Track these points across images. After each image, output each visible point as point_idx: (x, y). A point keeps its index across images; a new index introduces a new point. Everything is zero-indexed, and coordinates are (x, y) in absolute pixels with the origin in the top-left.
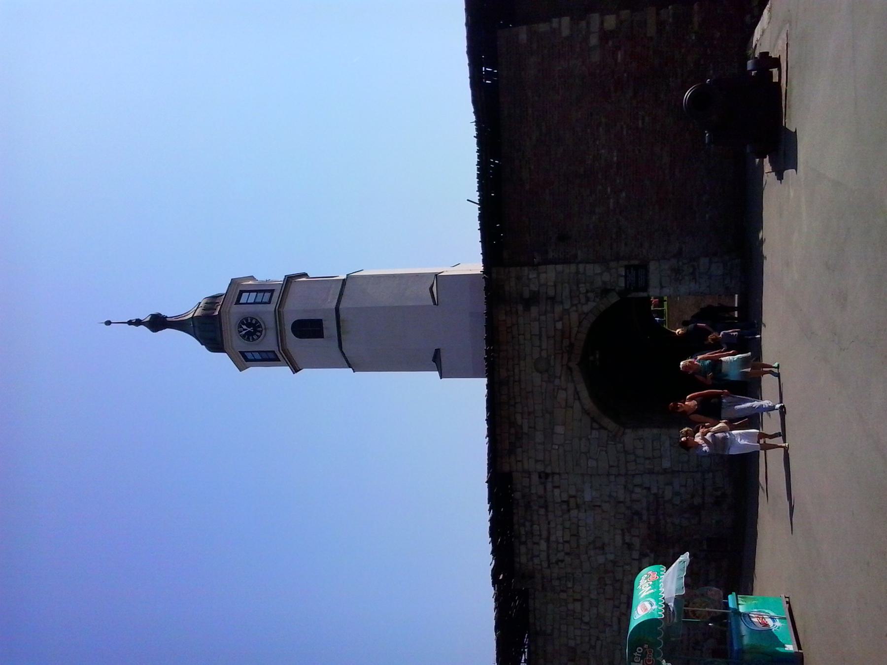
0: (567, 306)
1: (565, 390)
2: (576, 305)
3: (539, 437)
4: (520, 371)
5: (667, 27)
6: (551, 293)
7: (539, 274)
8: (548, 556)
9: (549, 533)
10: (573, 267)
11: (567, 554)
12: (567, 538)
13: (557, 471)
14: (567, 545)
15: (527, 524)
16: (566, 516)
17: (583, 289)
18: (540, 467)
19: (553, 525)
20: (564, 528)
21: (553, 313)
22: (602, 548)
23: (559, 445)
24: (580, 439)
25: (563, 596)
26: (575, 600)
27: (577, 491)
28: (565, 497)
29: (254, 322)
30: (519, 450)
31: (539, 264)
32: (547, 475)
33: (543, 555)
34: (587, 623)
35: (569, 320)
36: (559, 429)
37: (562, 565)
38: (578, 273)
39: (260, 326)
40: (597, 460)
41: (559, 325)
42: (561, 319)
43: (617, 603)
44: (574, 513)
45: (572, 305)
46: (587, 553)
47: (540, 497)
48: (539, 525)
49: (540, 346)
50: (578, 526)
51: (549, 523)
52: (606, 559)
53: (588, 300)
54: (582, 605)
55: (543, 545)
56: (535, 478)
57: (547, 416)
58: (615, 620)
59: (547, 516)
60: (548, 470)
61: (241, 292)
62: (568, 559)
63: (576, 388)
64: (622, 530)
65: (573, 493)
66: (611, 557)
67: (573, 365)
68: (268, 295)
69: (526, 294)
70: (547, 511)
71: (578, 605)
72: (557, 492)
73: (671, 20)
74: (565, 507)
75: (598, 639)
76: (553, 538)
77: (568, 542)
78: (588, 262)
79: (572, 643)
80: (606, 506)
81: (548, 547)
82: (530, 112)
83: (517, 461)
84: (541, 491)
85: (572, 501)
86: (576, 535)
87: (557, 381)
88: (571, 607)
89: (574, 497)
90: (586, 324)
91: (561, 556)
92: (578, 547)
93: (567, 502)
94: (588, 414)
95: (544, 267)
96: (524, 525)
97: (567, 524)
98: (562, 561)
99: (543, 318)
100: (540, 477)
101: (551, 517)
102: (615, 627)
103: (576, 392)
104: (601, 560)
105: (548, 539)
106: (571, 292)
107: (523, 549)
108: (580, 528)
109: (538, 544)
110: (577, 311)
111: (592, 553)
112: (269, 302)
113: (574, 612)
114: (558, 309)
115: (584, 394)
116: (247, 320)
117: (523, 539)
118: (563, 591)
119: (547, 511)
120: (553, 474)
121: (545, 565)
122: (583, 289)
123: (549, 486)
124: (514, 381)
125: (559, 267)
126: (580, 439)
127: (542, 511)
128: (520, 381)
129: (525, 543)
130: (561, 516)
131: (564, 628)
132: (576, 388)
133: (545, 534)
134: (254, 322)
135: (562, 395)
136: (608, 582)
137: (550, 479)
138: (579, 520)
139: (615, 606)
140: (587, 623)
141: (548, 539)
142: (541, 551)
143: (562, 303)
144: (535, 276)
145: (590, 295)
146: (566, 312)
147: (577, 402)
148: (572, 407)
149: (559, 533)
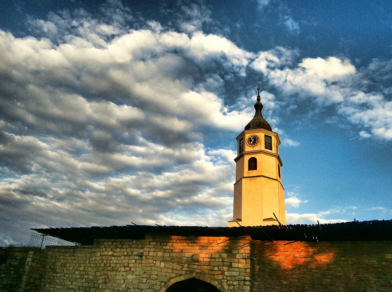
0: (226, 273)
1: (182, 270)
2: (227, 279)
3: (160, 254)
6: (234, 265)
7: (245, 259)
8: (105, 255)
9: (117, 256)
10: (248, 278)
11: (105, 265)
12: (112, 265)
13: (143, 262)
14: (109, 264)
15: (121, 246)
16: (122, 265)
17: (235, 283)
18: (145, 254)
19: (119, 258)
20: (116, 264)
21: (224, 266)
22: (106, 283)
23: (155, 264)
24: (157, 275)
25: (87, 262)
26: (85, 267)
27: (133, 272)
28: (131, 265)
29: (256, 142)
30: (154, 243)
31: (252, 260)
32: (141, 256)
33: (106, 253)
34: (74, 273)
35: (218, 274)
36: (163, 265)
37: (100, 262)
38: (245, 281)
39: (254, 144)
40: (146, 283)
41: (216, 268)
42: (219, 270)
43: (80, 288)
44: (123, 269)
45: (227, 276)
46: (104, 274)
47: (132, 252)
48: (120, 252)
49: (206, 258)
50: (116, 271)
51: (120, 257)
52: (100, 284)
53: (229, 285)
54: (82, 271)
55: (111, 253)
56: (141, 251)
57: (169, 259)
58: (74, 287)
60: (144, 257)
61: (271, 137)
62: (102, 265)
63: (181, 275)
65: (133, 269)
66: (101, 286)
67: (194, 275)
69: (234, 252)
70: (126, 256)
71: (82, 269)
72: (134, 261)
74: (126, 265)
75: (67, 278)
76: (113, 258)
77: (110, 266)
78: (251, 287)
79: (68, 265)
80: (124, 286)
81: (109, 255)
82: (343, 259)
83: (149, 242)
84: (135, 253)
85: (128, 269)
86: (113, 270)
87: (186, 265)
88: (82, 265)
89: (130, 270)
91: (105, 262)
92: (108, 270)
93: (128, 266)
94: (168, 281)
95: (249, 262)
96: (120, 245)
97: (118, 266)
98: (102, 262)
99: (221, 260)
100: (142, 253)
101: (123, 257)
102: (71, 287)
103: (180, 275)
104: (100, 281)
105: (112, 255)
106: (235, 276)
107: (110, 243)
108: (115, 272)
109: (111, 250)
110: (223, 279)
111: (103, 277)
113: (80, 267)
114: (225, 268)
115: (178, 279)
116: (257, 139)
117: (115, 244)
118: (89, 261)
119: (126, 256)
120: (142, 260)
121: (102, 254)
122: (235, 283)
123: (137, 258)
124: (188, 243)
125: (248, 271)
126: (157, 275)
127: (126, 253)
129: (113, 244)
130: (122, 263)
131: (74, 262)
133: (115, 254)
135: (179, 267)
136: (90, 284)
137: (140, 258)
138: (119, 271)
139: (79, 287)
140: (74, 273)
141: (112, 255)
142: (108, 252)
143: (228, 271)
144: (244, 257)
145: (232, 287)
146: (223, 273)
147: (174, 275)
148: (173, 273)
149: (115, 261)
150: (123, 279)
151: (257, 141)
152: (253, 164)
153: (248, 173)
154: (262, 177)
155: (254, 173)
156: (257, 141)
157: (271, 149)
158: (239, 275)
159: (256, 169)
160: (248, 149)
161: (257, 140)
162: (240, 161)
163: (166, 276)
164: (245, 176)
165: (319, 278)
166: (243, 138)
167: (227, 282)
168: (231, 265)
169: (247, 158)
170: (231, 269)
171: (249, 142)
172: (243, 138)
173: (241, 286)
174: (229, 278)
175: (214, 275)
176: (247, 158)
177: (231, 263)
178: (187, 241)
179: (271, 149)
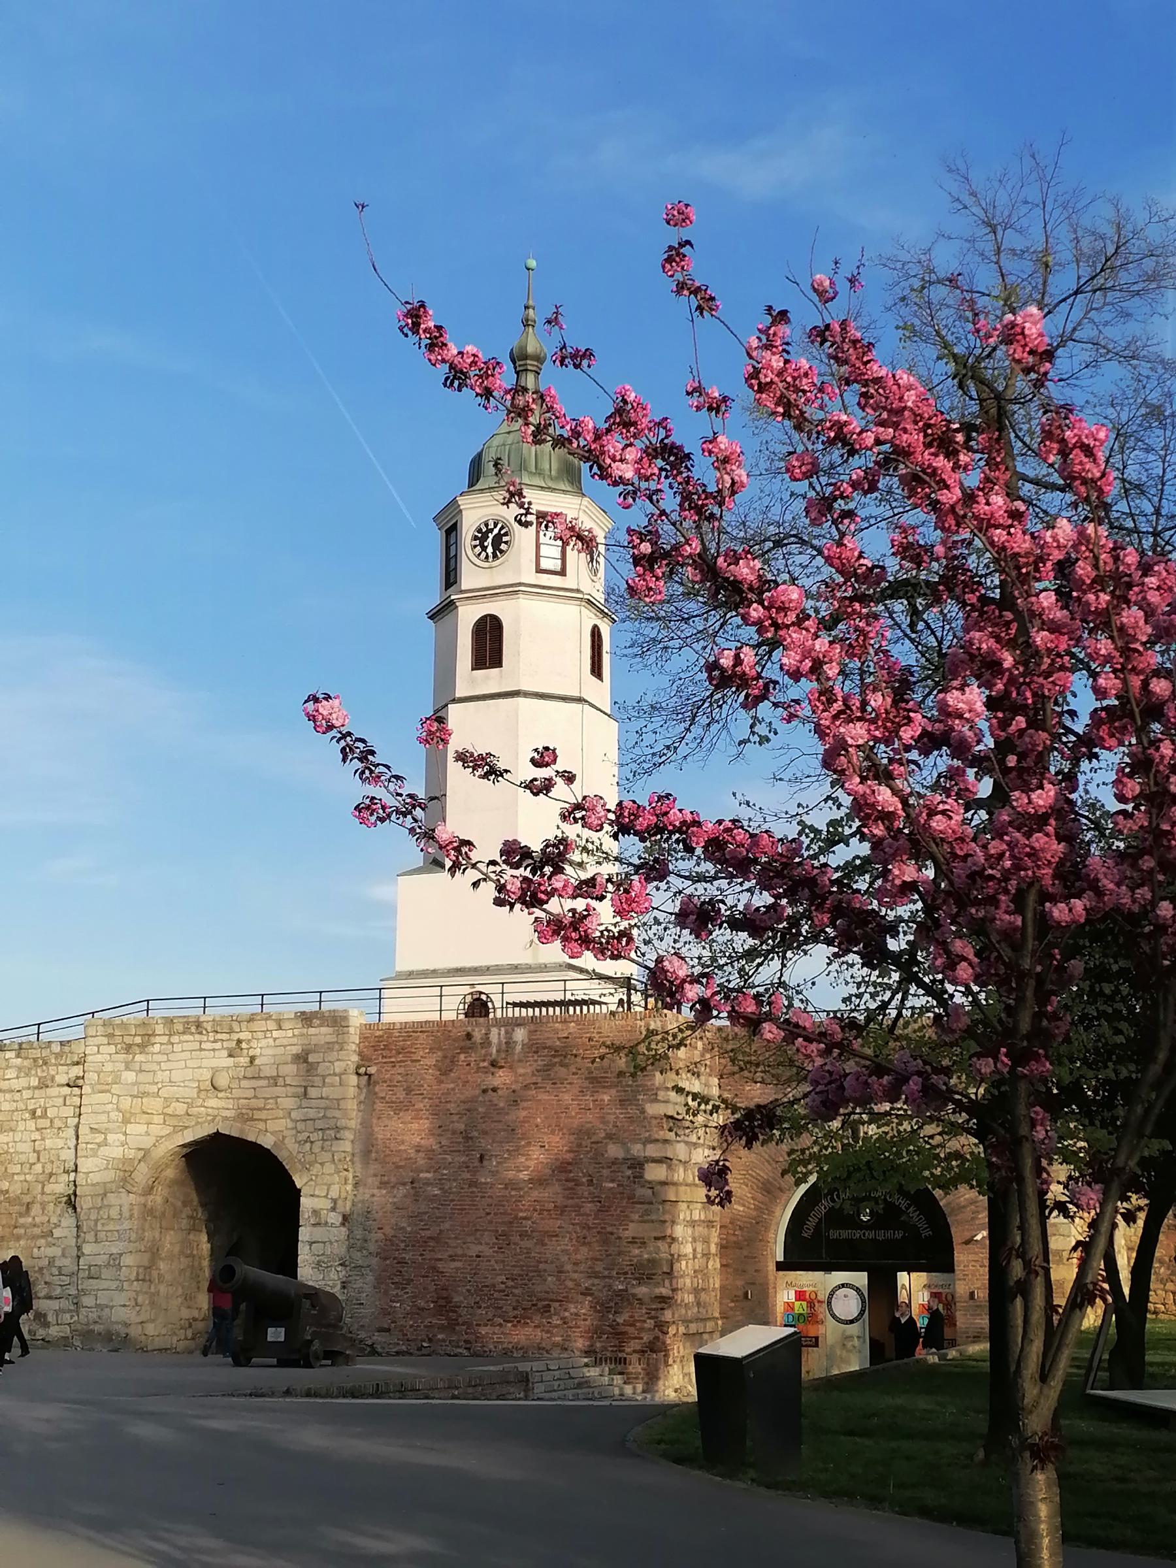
0: (294, 1115)
4: (214, 1050)
5: (637, 1251)
6: (313, 1092)
19: (17, 1096)
29: (503, 547)
59: (29, 1088)
63: (186, 1127)
64: (7, 1191)
68: (556, 565)
70: (36, 1088)
73: (646, 1256)
83: (98, 1046)
90: (267, 1142)
94: (154, 1145)
112: (539, 570)
116: (506, 534)
127: (34, 1082)
128: (201, 1050)
132: (186, 1127)
134: (503, 547)
143: (300, 1107)
150: (34, 1151)
151: (506, 543)
152: (489, 643)
153: (473, 681)
154: (521, 700)
155: (490, 680)
156: (506, 543)
157: (562, 572)
158: (324, 1117)
159: (499, 664)
160: (472, 575)
161: (505, 539)
162: (448, 618)
163: (147, 1134)
164: (459, 694)
165: (503, 1109)
166: (456, 524)
167: (295, 1136)
168: (305, 1094)
169: (468, 615)
170: (305, 1103)
171: (475, 546)
172: (456, 524)
173: (329, 1143)
174: (300, 1126)
175: (265, 1121)
176: (468, 615)
177: (306, 1088)
178: (197, 1037)
179: (562, 572)
